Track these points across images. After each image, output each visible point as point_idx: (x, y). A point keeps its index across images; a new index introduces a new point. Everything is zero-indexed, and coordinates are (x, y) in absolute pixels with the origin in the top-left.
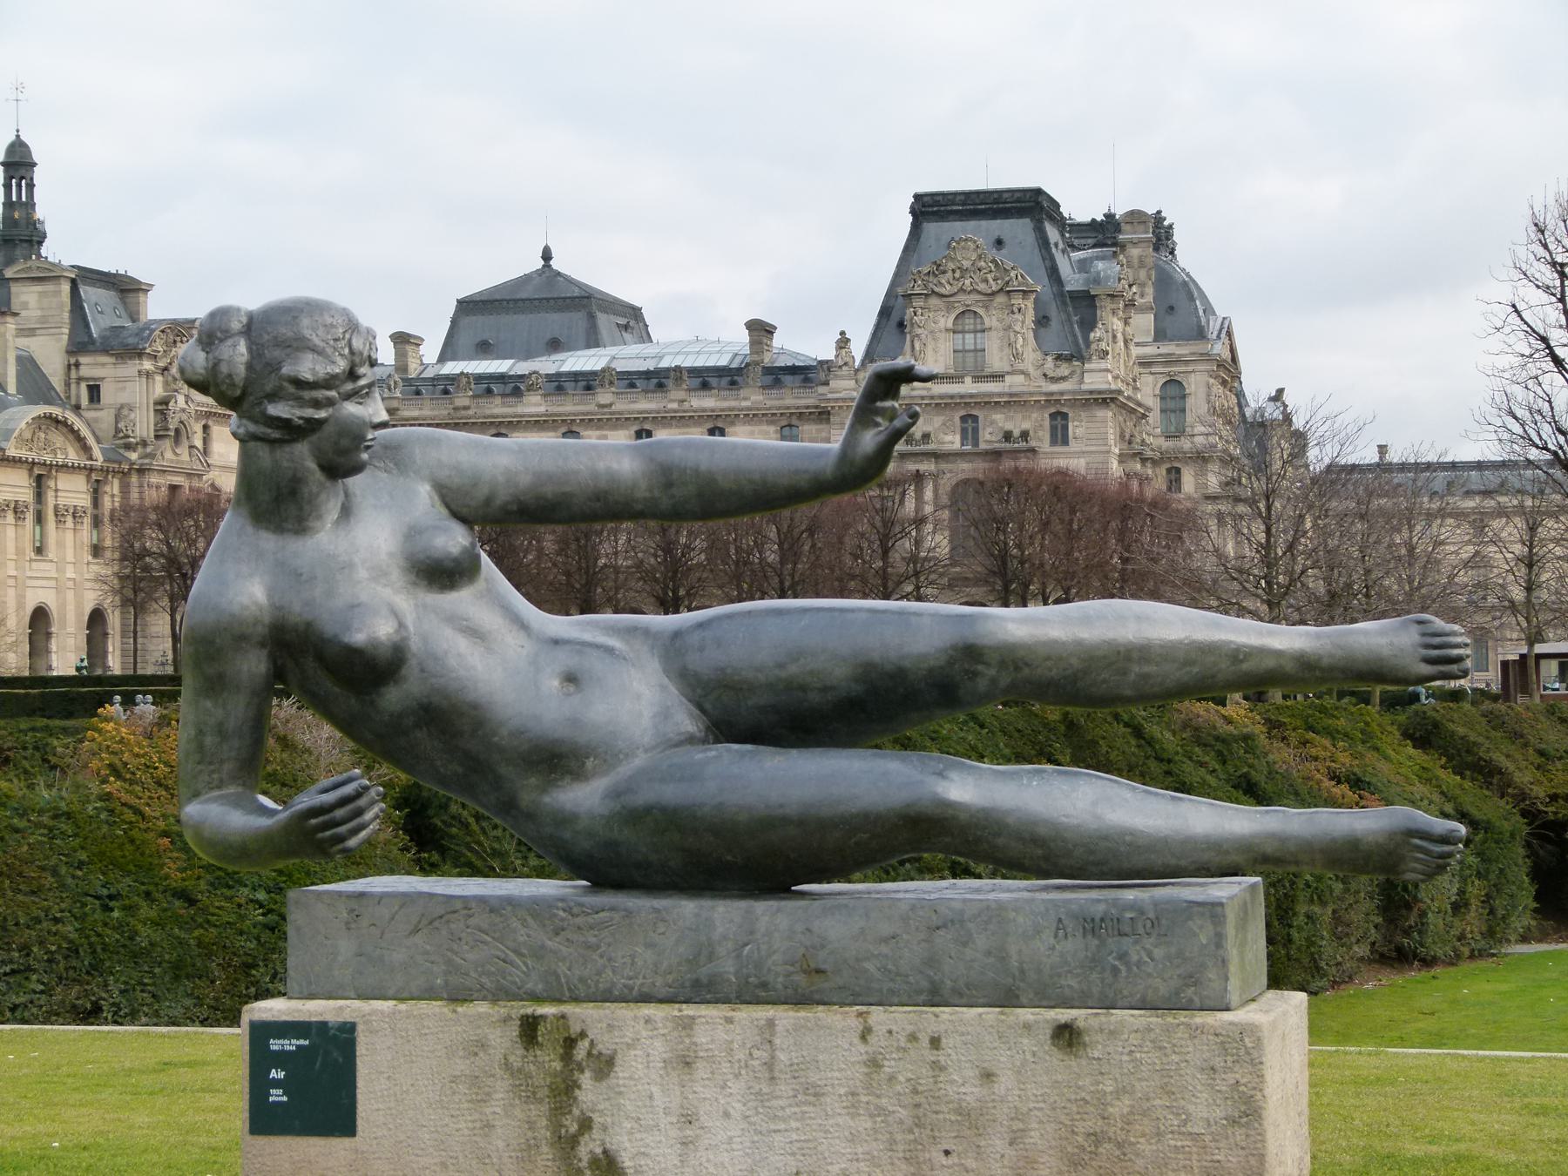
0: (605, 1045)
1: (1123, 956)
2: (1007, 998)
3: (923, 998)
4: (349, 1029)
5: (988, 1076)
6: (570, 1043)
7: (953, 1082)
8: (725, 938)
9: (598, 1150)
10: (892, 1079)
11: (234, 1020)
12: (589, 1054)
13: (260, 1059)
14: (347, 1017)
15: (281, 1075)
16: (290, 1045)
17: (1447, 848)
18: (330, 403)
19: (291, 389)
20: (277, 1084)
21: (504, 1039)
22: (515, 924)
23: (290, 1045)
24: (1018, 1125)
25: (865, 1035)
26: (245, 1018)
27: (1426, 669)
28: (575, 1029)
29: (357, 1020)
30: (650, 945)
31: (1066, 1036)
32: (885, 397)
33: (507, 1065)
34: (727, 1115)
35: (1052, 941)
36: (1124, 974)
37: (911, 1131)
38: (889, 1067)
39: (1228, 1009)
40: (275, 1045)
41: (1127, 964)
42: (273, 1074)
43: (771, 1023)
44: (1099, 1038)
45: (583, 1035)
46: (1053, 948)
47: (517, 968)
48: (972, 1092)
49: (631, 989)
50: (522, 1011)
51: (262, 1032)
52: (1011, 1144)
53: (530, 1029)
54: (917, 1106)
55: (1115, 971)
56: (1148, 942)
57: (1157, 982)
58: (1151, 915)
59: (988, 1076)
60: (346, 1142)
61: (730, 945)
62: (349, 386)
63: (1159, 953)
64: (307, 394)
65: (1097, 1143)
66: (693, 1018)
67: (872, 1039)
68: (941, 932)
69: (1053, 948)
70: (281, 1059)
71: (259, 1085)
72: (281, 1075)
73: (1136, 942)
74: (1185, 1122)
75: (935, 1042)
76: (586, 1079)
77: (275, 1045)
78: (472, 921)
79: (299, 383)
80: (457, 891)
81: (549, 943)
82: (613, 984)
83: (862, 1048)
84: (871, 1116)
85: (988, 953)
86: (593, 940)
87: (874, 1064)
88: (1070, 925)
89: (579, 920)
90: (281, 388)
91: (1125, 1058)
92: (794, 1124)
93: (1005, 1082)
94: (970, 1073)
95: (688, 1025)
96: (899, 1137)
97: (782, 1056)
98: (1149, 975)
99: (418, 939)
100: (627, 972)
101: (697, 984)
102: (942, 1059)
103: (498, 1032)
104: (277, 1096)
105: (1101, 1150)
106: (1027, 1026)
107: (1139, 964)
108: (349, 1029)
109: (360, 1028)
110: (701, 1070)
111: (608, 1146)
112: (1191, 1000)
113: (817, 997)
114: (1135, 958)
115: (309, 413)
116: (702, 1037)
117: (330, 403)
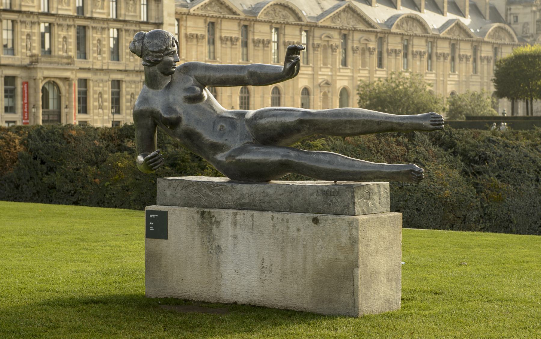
0: (218, 220)
1: (331, 201)
2: (306, 211)
3: (288, 210)
5: (298, 230)
6: (211, 218)
7: (291, 231)
8: (246, 193)
9: (217, 245)
10: (278, 230)
11: (142, 209)
12: (215, 221)
13: (148, 220)
14: (166, 210)
15: (152, 224)
17: (420, 175)
18: (161, 56)
19: (151, 53)
20: (151, 226)
21: (197, 216)
22: (203, 189)
24: (305, 243)
25: (273, 218)
26: (146, 209)
27: (431, 127)
28: (213, 214)
30: (231, 195)
31: (316, 221)
32: (294, 54)
33: (198, 223)
34: (243, 237)
35: (316, 196)
36: (332, 205)
37: (282, 244)
38: (277, 227)
39: (354, 215)
40: (151, 216)
41: (332, 203)
43: (253, 215)
44: (322, 221)
45: (214, 216)
46: (316, 198)
47: (203, 199)
48: (296, 234)
49: (227, 205)
50: (202, 210)
51: (149, 213)
52: (303, 247)
53: (203, 214)
54: (283, 237)
55: (330, 205)
56: (337, 197)
57: (339, 208)
58: (338, 190)
59: (298, 230)
60: (165, 240)
61: (247, 195)
62: (166, 52)
63: (339, 200)
64: (155, 54)
65: (322, 248)
66: (237, 213)
67: (274, 220)
68: (292, 193)
69: (316, 198)
71: (148, 226)
72: (152, 224)
73: (334, 197)
74: (341, 243)
75: (288, 221)
76: (214, 227)
77: (151, 216)
78: (195, 187)
79: (152, 52)
80: (202, 180)
81: (210, 194)
82: (223, 204)
83: (272, 222)
84: (274, 239)
85: (302, 199)
86: (219, 193)
87: (274, 226)
88: (320, 192)
89: (216, 188)
90: (149, 53)
91: (328, 227)
92: (258, 241)
93: (302, 232)
94: (295, 229)
95: (235, 214)
96: (280, 245)
97: (254, 223)
98: (337, 206)
99: (183, 191)
100: (226, 201)
101: (240, 205)
102: (289, 225)
103: (196, 215)
104: (152, 229)
105: (323, 250)
106: (307, 218)
107: (335, 202)
109: (168, 213)
110: (238, 227)
111: (219, 245)
112: (346, 213)
113: (266, 209)
114: (334, 201)
115: (155, 59)
116: (238, 217)
117: (161, 56)
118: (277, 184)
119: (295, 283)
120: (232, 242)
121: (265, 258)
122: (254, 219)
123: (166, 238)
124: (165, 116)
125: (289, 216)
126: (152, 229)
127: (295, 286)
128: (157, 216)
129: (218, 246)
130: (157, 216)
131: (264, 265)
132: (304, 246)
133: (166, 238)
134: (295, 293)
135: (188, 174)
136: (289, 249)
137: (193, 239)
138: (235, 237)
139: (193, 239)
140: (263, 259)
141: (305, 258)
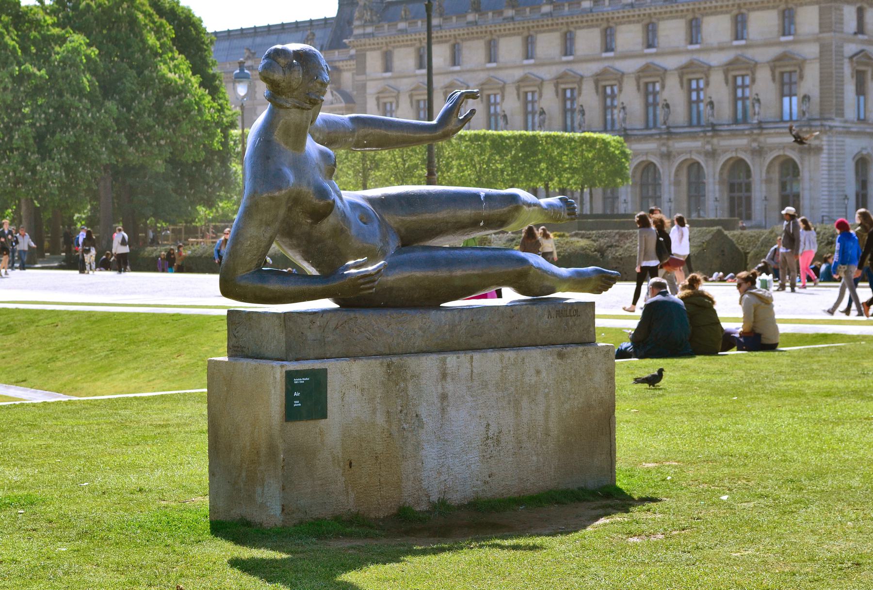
4: (324, 372)
5: (538, 372)
15: (299, 394)
16: (302, 381)
20: (297, 398)
23: (302, 381)
24: (547, 390)
29: (284, 371)
31: (561, 356)
42: (295, 394)
59: (538, 372)
70: (299, 387)
72: (299, 394)
93: (544, 374)
97: (475, 371)
108: (324, 372)
110: (449, 379)
118: (314, 313)
119: (533, 452)
120: (439, 405)
121: (490, 423)
122: (473, 364)
123: (324, 416)
124: (322, 203)
125: (523, 353)
126: (297, 404)
127: (535, 458)
128: (307, 379)
129: (417, 416)
130: (307, 379)
131: (489, 434)
132: (546, 395)
133: (324, 416)
134: (533, 468)
135: (58, 316)
136: (525, 402)
137: (374, 411)
138: (444, 397)
139: (374, 411)
140: (489, 425)
141: (547, 414)
